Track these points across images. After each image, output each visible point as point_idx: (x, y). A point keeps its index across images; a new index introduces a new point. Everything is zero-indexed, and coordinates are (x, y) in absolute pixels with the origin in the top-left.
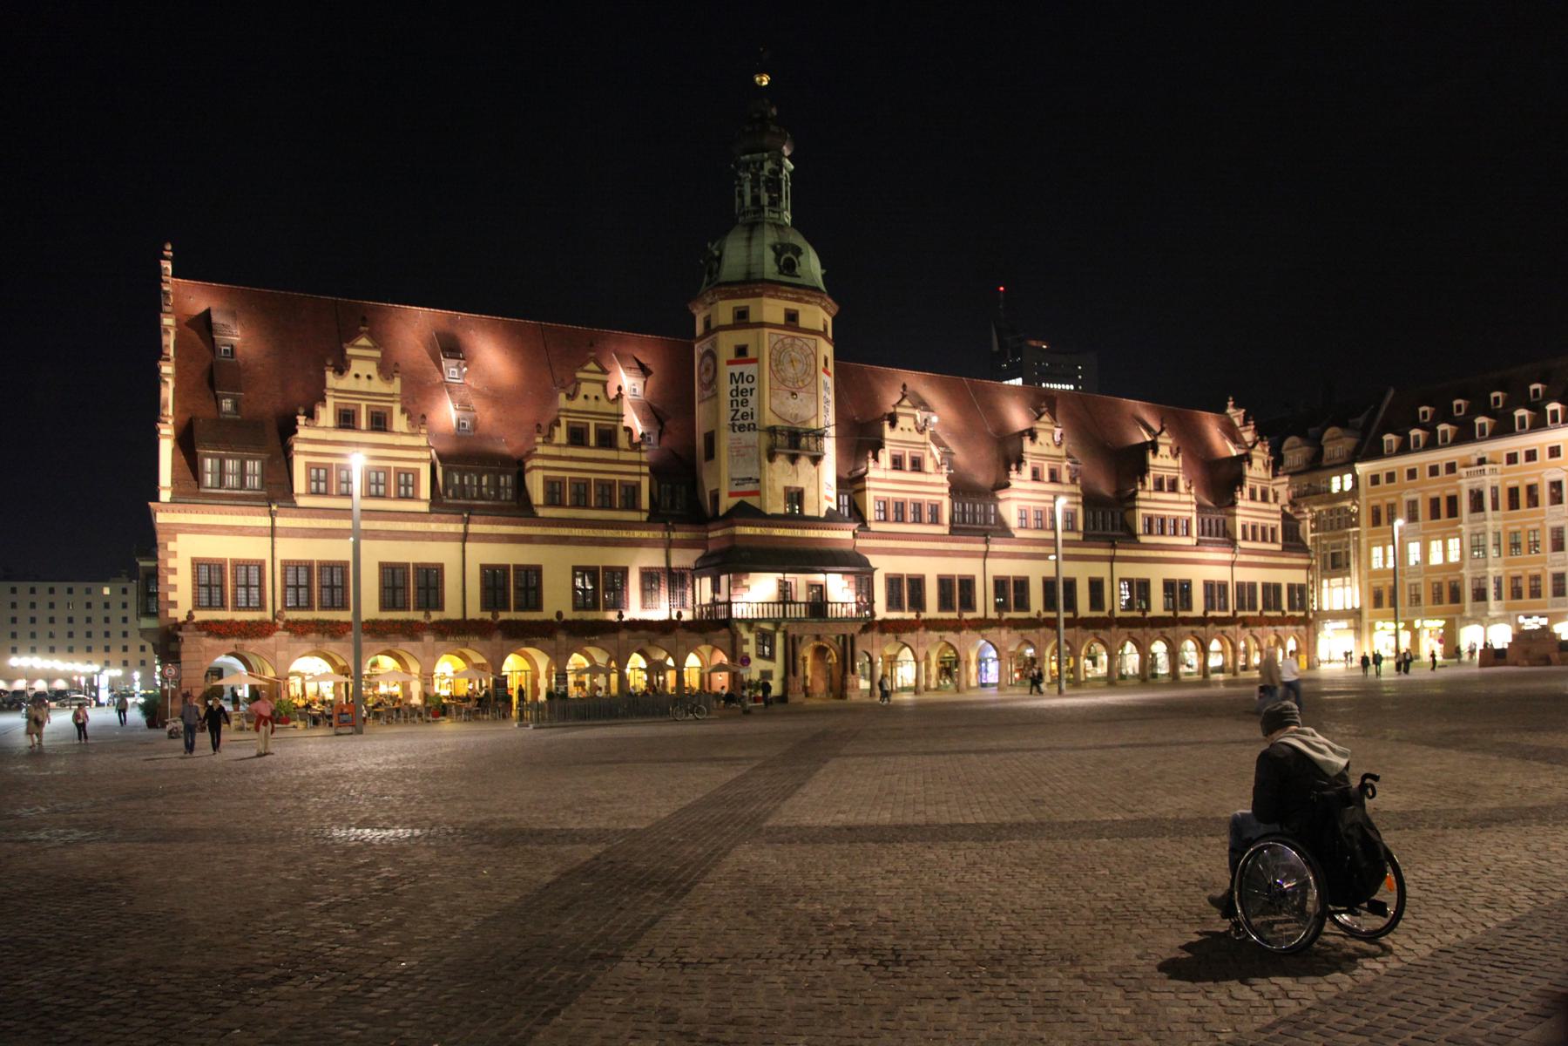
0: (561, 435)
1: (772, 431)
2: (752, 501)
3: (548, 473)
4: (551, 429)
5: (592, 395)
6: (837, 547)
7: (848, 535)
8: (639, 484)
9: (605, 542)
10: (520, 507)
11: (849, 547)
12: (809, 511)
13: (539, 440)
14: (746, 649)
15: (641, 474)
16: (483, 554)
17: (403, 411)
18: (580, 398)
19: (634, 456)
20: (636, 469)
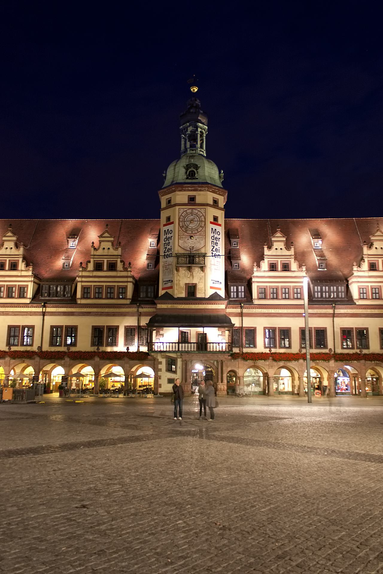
0: (91, 266)
1: (178, 256)
2: (169, 291)
3: (83, 284)
4: (87, 264)
5: (106, 248)
6: (215, 314)
7: (223, 306)
8: (127, 286)
9: (108, 314)
10: (72, 301)
11: (222, 313)
12: (199, 295)
13: (81, 269)
14: (160, 366)
15: (127, 282)
16: (50, 321)
17: (23, 262)
18: (101, 249)
19: (124, 274)
20: (125, 279)
